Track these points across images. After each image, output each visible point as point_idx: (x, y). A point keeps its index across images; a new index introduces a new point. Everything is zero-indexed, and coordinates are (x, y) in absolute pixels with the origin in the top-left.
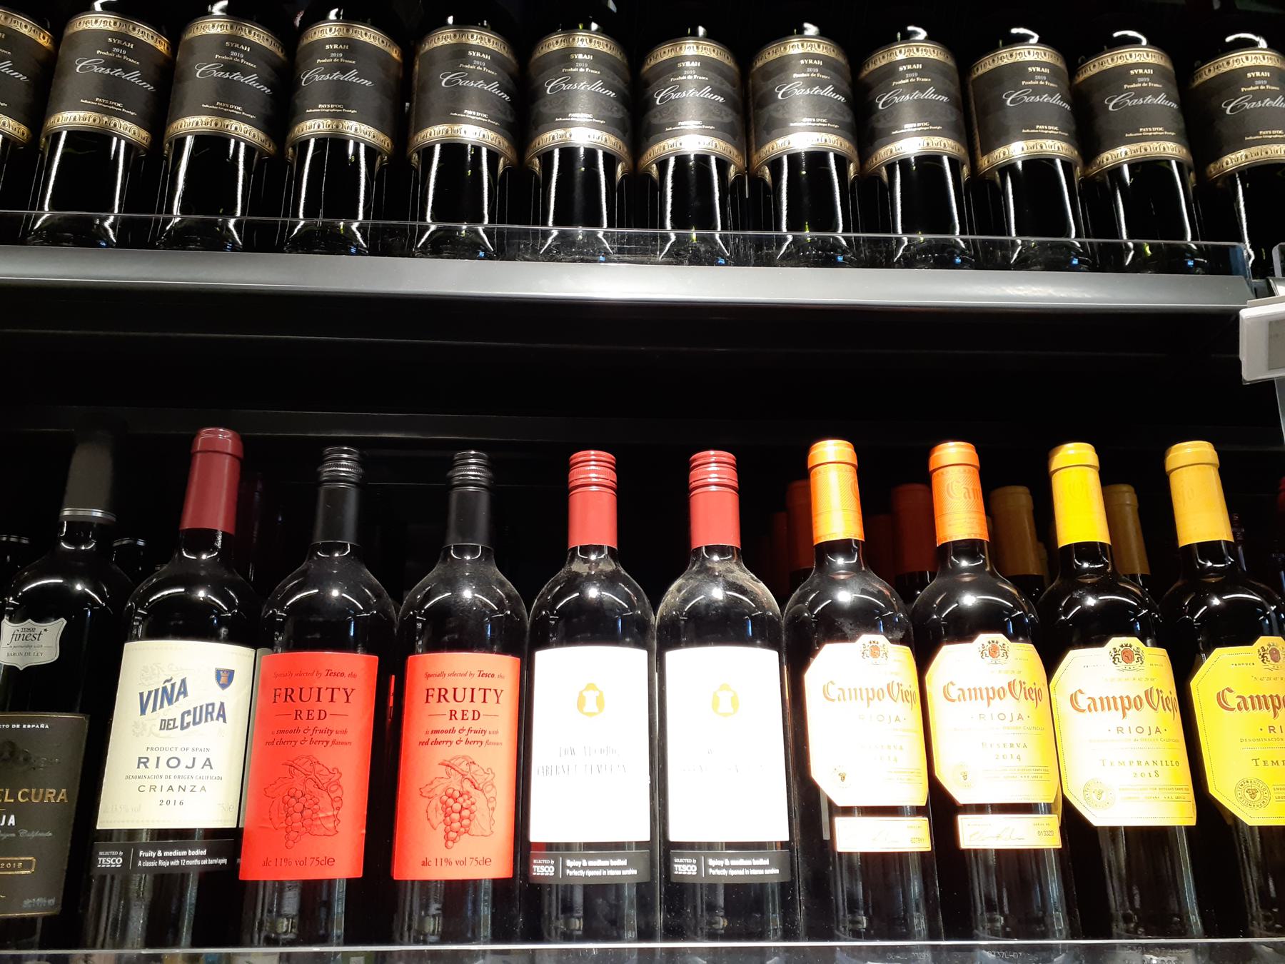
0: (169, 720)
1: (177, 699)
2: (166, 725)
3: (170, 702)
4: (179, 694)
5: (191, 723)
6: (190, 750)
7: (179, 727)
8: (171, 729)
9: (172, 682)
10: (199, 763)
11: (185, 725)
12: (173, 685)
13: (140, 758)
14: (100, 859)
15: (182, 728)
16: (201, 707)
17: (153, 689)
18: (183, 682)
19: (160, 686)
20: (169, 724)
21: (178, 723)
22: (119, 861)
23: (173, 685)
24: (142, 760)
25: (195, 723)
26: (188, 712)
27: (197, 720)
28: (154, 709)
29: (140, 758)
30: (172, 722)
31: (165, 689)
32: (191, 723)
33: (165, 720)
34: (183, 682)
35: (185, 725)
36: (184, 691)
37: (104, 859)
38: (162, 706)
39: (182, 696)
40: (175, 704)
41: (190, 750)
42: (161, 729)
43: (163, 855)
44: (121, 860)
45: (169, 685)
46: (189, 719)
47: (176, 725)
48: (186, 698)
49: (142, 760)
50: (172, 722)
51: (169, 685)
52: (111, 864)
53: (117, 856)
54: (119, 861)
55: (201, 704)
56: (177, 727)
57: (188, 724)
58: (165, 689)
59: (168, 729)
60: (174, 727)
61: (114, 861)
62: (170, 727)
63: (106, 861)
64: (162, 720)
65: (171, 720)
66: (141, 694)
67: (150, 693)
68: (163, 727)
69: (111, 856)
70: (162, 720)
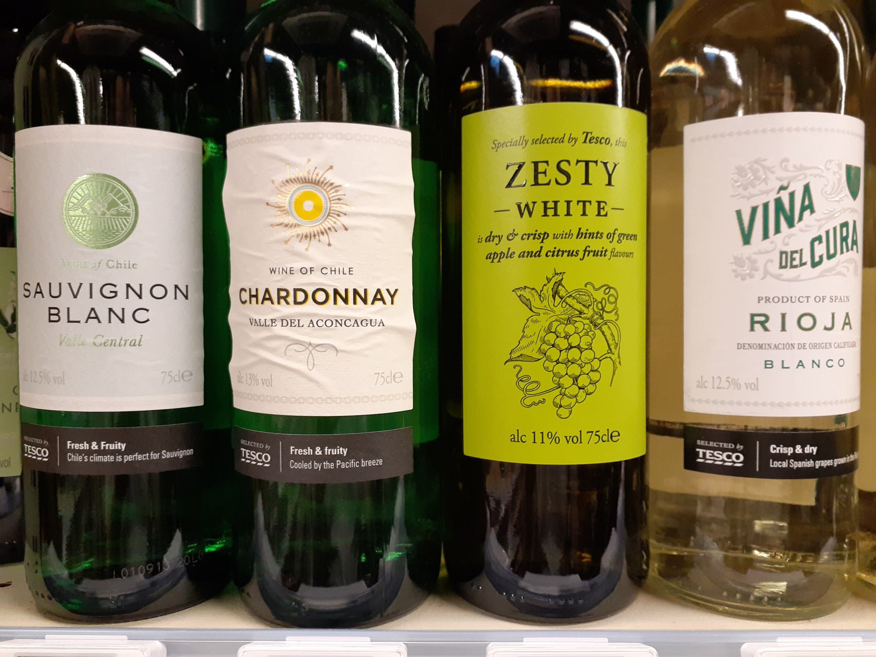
0: (793, 252)
1: (800, 219)
2: (788, 260)
3: (791, 225)
4: (803, 209)
5: (825, 257)
6: (828, 300)
7: (809, 263)
8: (796, 267)
9: (790, 190)
10: (839, 322)
11: (817, 259)
12: (792, 195)
13: (753, 316)
14: (701, 451)
15: (814, 265)
16: (835, 229)
17: (759, 202)
18: (807, 189)
19: (771, 198)
20: (793, 259)
21: (807, 258)
22: (738, 457)
23: (792, 195)
24: (757, 319)
25: (830, 257)
26: (819, 239)
27: (832, 251)
28: (766, 236)
29: (753, 316)
30: (797, 256)
31: (778, 202)
32: (825, 257)
33: (786, 253)
34: (807, 189)
35: (817, 259)
36: (808, 206)
37: (708, 452)
38: (778, 230)
39: (807, 213)
40: (798, 226)
41: (828, 300)
42: (781, 267)
43: (803, 451)
44: (742, 458)
45: (785, 197)
46: (820, 249)
47: (804, 261)
48: (814, 215)
49: (757, 319)
50: (797, 256)
51: (785, 197)
52: (723, 461)
53: (734, 451)
54: (738, 457)
55: (834, 226)
56: (805, 264)
57: (821, 257)
58: (778, 202)
59: (792, 267)
60: (802, 264)
61: (729, 457)
62: (795, 263)
63: (713, 456)
64: (782, 253)
65: (796, 252)
66: (739, 213)
67: (754, 210)
68: (784, 264)
69: (724, 450)
70: (782, 253)
